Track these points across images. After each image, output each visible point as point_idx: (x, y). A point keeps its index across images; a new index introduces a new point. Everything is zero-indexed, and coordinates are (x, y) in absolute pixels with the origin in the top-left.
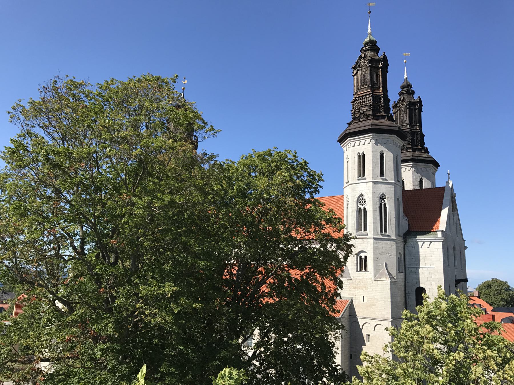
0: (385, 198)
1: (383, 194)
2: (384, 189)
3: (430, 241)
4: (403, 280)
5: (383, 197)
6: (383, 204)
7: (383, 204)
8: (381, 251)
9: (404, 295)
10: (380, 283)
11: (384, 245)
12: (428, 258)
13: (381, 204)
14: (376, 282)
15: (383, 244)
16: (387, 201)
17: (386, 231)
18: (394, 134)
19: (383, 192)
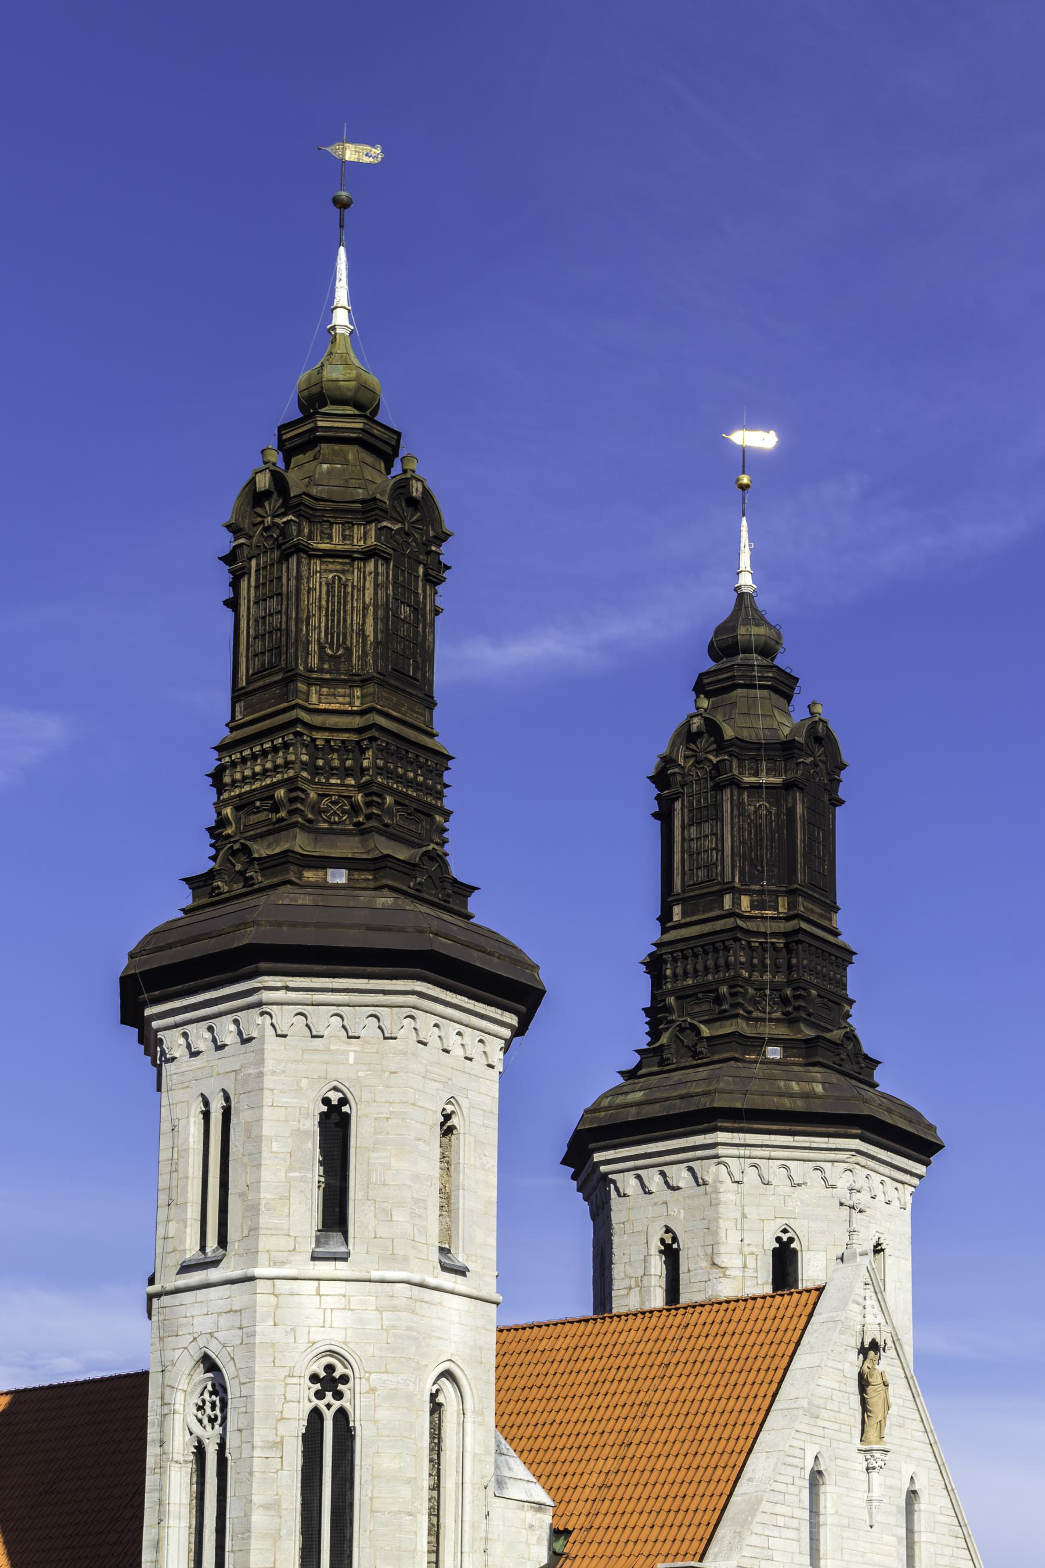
1: (332, 1353)
7: (329, 1416)
13: (316, 1416)
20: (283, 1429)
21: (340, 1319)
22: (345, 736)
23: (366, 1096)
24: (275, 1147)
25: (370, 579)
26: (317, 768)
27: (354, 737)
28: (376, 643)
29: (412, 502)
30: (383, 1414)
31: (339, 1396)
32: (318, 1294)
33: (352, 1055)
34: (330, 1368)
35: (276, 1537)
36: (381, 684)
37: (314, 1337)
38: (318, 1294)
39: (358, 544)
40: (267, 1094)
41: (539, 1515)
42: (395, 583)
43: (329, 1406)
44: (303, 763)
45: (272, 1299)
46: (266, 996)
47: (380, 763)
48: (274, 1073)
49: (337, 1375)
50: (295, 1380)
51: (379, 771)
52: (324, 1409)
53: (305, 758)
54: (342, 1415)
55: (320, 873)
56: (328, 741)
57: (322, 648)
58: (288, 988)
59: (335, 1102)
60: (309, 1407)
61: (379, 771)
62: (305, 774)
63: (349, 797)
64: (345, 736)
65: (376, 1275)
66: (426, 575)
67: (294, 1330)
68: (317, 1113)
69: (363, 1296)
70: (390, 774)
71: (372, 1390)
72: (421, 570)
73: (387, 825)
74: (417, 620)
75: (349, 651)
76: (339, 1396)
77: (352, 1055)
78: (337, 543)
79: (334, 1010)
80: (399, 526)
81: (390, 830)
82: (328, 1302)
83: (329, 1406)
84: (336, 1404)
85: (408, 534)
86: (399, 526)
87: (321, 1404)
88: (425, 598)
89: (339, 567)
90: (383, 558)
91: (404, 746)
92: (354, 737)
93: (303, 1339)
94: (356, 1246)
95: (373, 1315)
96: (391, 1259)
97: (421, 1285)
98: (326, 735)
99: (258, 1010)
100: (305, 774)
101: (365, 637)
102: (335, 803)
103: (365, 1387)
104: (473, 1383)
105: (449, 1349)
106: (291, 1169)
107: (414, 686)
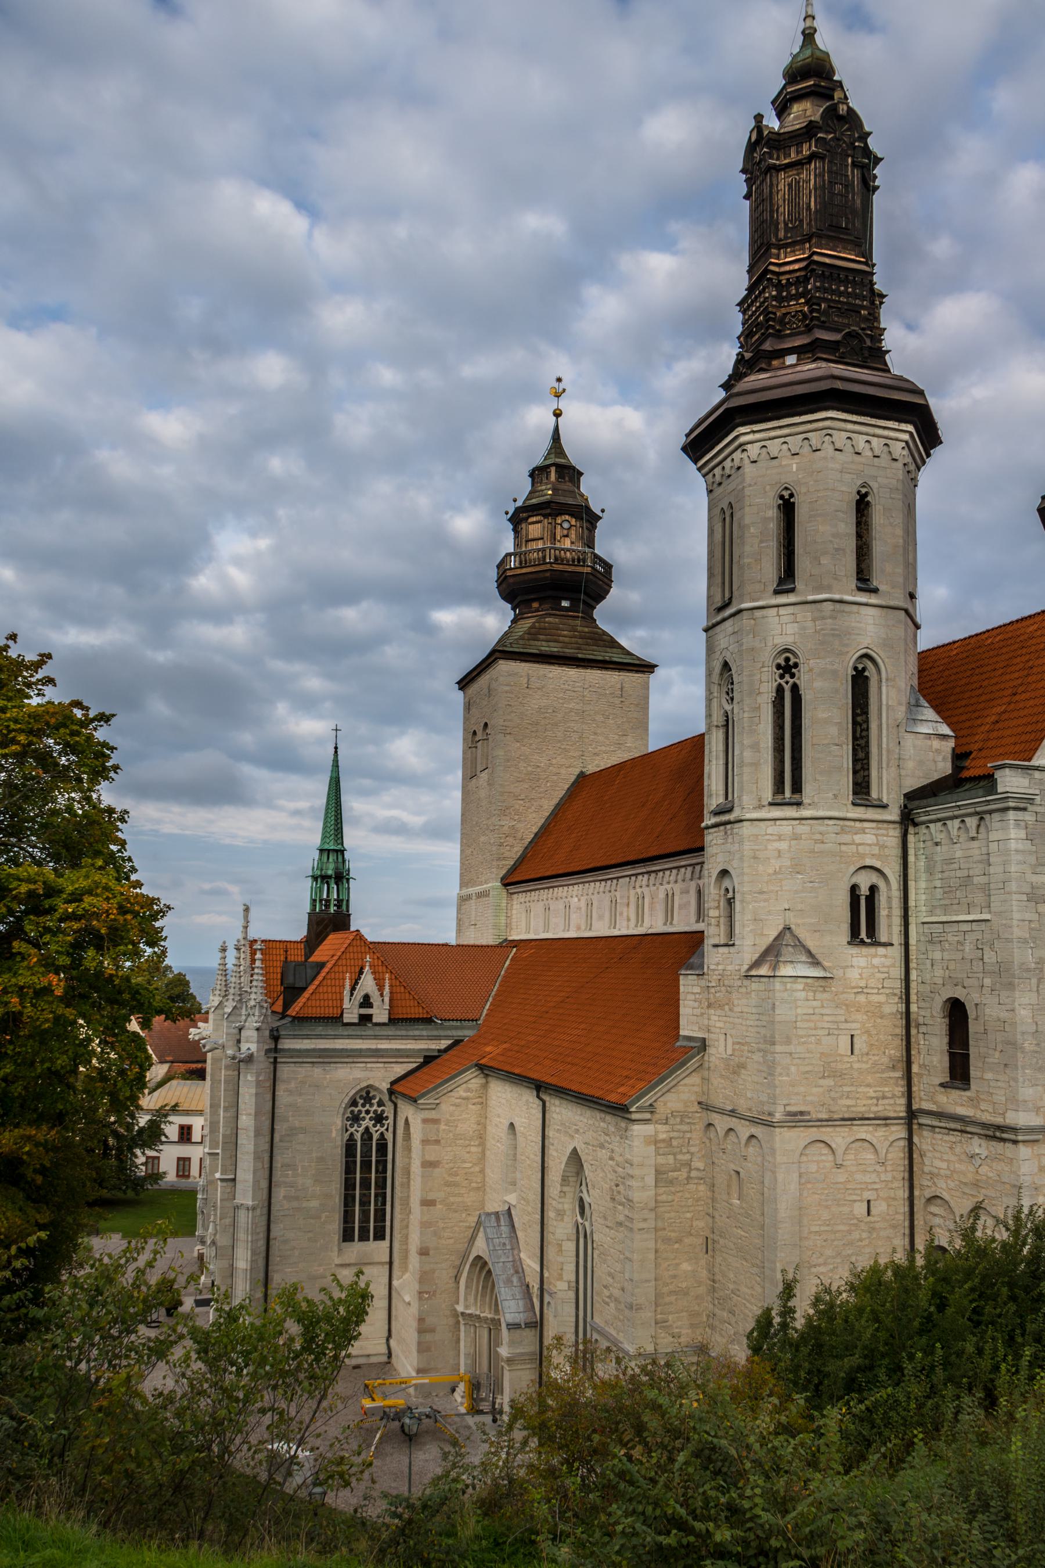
0: (796, 665)
1: (787, 650)
2: (792, 628)
3: (977, 813)
4: (898, 972)
5: (787, 659)
6: (787, 688)
7: (787, 688)
8: (775, 864)
9: (900, 1031)
10: (755, 985)
11: (784, 845)
12: (976, 880)
14: (746, 982)
15: (780, 838)
16: (803, 678)
17: (797, 788)
18: (826, 409)
19: (781, 641)
20: (759, 699)
21: (792, 628)
22: (798, 274)
23: (804, 490)
24: (752, 530)
25: (812, 173)
26: (783, 298)
27: (803, 273)
28: (816, 210)
29: (841, 118)
30: (818, 684)
31: (793, 676)
32: (778, 615)
33: (794, 466)
34: (787, 659)
35: (756, 765)
36: (820, 236)
37: (776, 641)
38: (778, 615)
39: (806, 152)
40: (747, 498)
41: (944, 743)
42: (830, 172)
43: (787, 683)
44: (773, 296)
45: (752, 622)
46: (743, 439)
47: (818, 284)
48: (750, 485)
49: (783, 663)
50: (766, 669)
51: (817, 289)
52: (784, 684)
53: (774, 293)
54: (795, 688)
55: (781, 360)
56: (788, 280)
57: (786, 224)
58: (754, 432)
59: (787, 497)
60: (775, 684)
61: (817, 289)
62: (774, 303)
63: (801, 311)
64: (798, 274)
65: (810, 598)
66: (853, 162)
67: (765, 639)
68: (775, 505)
69: (805, 614)
70: (825, 290)
71: (811, 670)
72: (850, 160)
73: (824, 322)
74: (847, 192)
75: (801, 221)
76: (793, 676)
77: (794, 466)
78: (793, 156)
79: (783, 440)
80: (831, 136)
81: (827, 325)
82: (784, 619)
83: (787, 683)
84: (791, 681)
85: (838, 140)
86: (831, 136)
87: (782, 682)
88: (853, 177)
89: (795, 172)
90: (820, 158)
91: (835, 271)
92: (803, 273)
93: (770, 644)
94: (799, 585)
95: (810, 624)
96: (819, 589)
97: (841, 602)
98: (788, 276)
99: (739, 450)
100: (774, 303)
101: (810, 210)
102: (793, 317)
103: (807, 669)
104: (886, 660)
105: (866, 641)
106: (761, 542)
107: (847, 234)
